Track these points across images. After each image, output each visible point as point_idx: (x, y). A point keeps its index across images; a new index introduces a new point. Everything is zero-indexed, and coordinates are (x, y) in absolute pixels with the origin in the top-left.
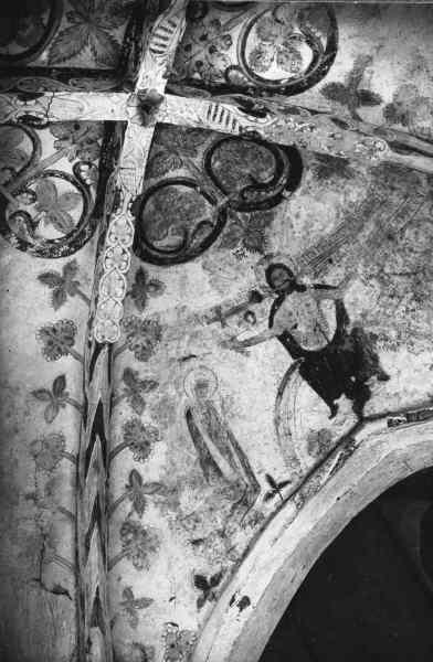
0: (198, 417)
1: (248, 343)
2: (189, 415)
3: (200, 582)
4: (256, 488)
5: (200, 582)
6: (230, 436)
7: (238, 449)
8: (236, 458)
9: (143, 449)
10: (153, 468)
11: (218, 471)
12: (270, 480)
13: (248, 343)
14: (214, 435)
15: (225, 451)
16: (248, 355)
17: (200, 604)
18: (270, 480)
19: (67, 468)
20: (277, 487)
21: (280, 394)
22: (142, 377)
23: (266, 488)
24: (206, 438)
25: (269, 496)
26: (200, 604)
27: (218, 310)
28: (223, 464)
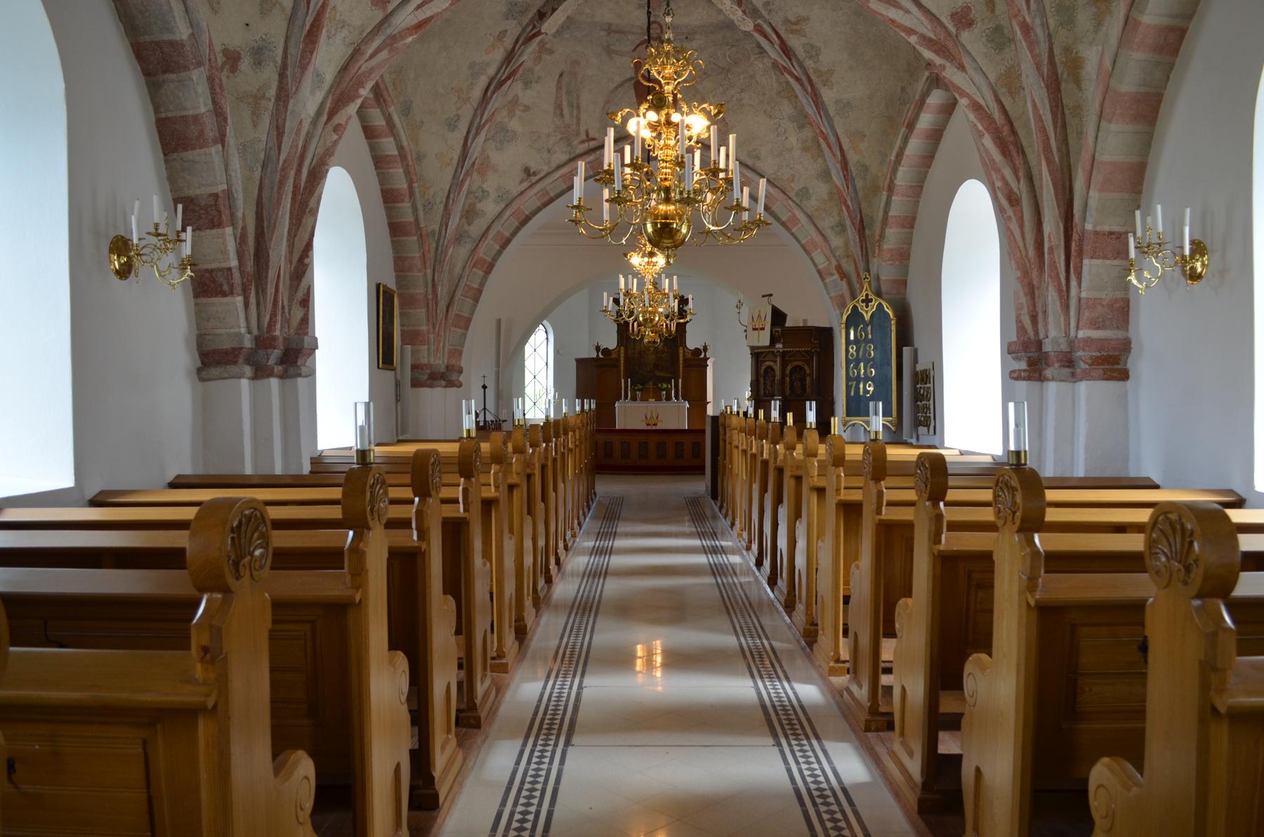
0: (565, 79)
1: (616, 52)
2: (561, 75)
3: (528, 172)
4: (578, 134)
5: (528, 172)
6: (578, 97)
7: (578, 107)
8: (575, 113)
9: (527, 84)
10: (527, 97)
11: (562, 115)
12: (587, 134)
13: (616, 52)
14: (569, 93)
15: (571, 105)
16: (611, 58)
17: (521, 182)
18: (587, 134)
19: (483, 81)
20: (589, 139)
21: (617, 88)
22: (548, 46)
23: (583, 137)
24: (564, 91)
25: (583, 142)
26: (521, 182)
27: (610, 25)
28: (566, 111)
